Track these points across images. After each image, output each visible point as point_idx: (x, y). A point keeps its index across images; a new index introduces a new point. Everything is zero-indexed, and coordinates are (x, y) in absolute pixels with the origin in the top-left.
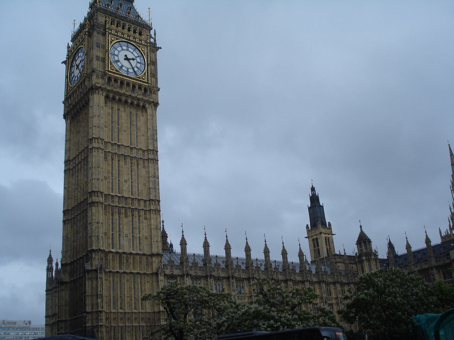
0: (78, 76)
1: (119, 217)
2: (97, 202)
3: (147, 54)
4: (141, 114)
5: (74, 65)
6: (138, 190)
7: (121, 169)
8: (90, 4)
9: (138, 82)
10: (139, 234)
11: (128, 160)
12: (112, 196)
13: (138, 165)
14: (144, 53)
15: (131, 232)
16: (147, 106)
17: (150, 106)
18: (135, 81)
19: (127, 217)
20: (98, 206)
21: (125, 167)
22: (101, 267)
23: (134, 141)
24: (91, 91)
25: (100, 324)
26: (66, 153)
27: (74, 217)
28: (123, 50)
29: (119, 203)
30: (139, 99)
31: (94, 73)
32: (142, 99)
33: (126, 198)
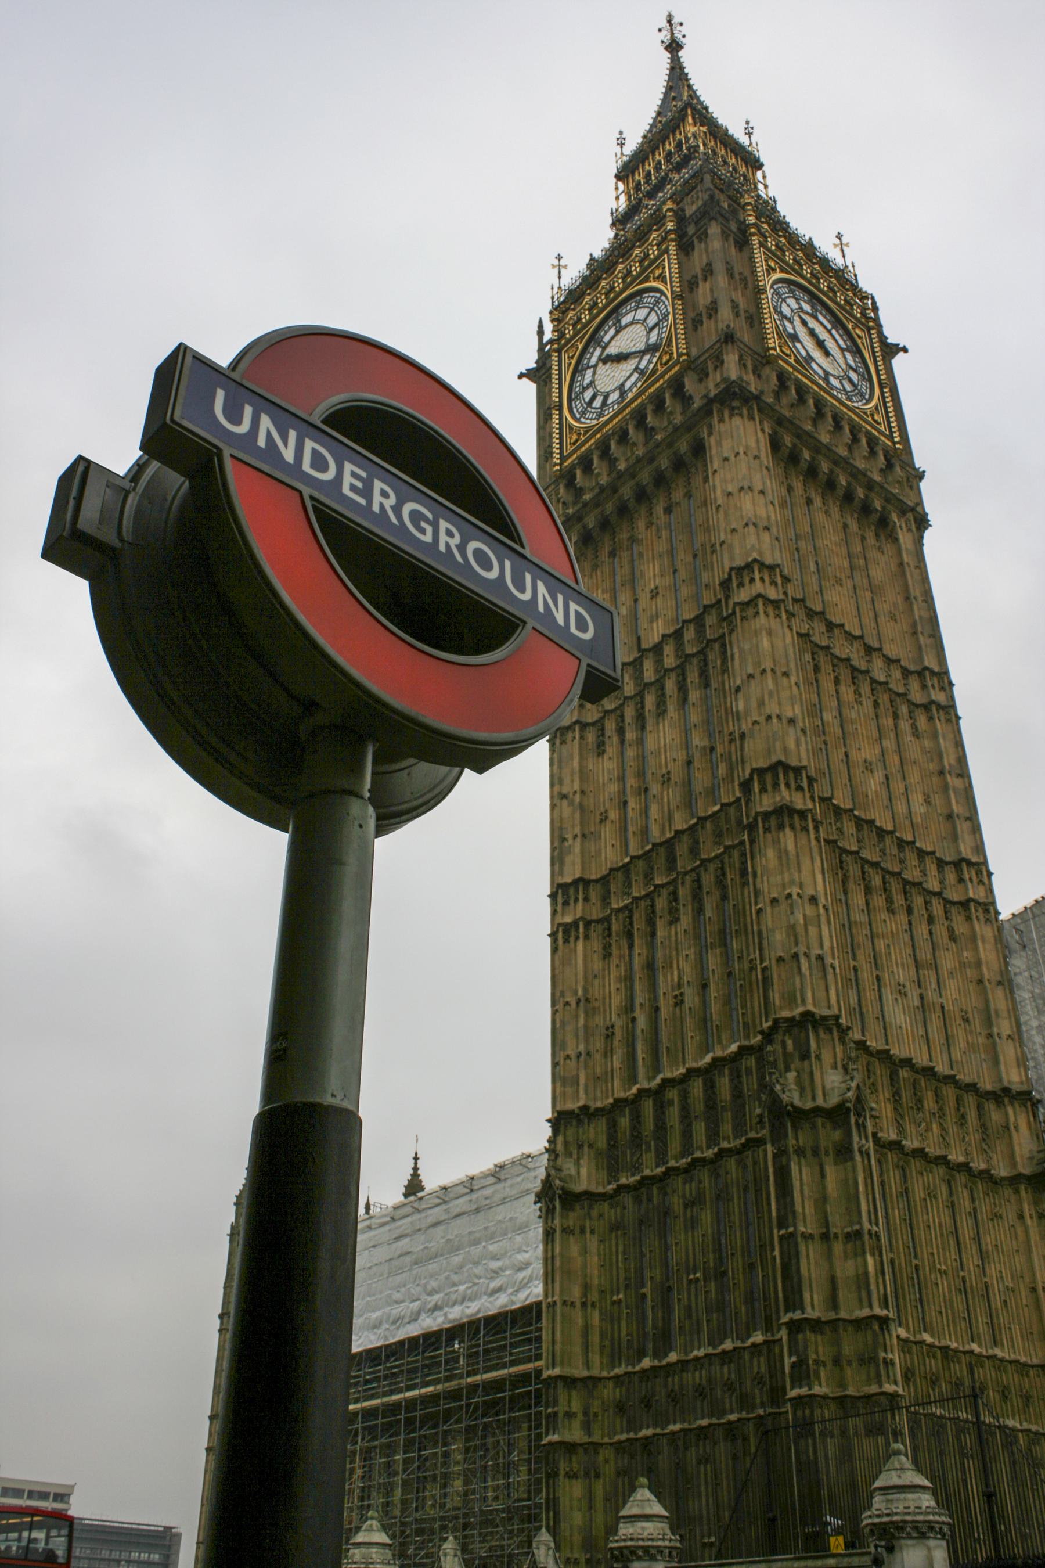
0: (623, 385)
8: (612, 214)
11: (865, 688)
13: (896, 716)
16: (894, 517)
17: (903, 520)
18: (856, 419)
20: (805, 829)
22: (859, 1099)
30: (870, 485)
31: (730, 345)
33: (881, 833)
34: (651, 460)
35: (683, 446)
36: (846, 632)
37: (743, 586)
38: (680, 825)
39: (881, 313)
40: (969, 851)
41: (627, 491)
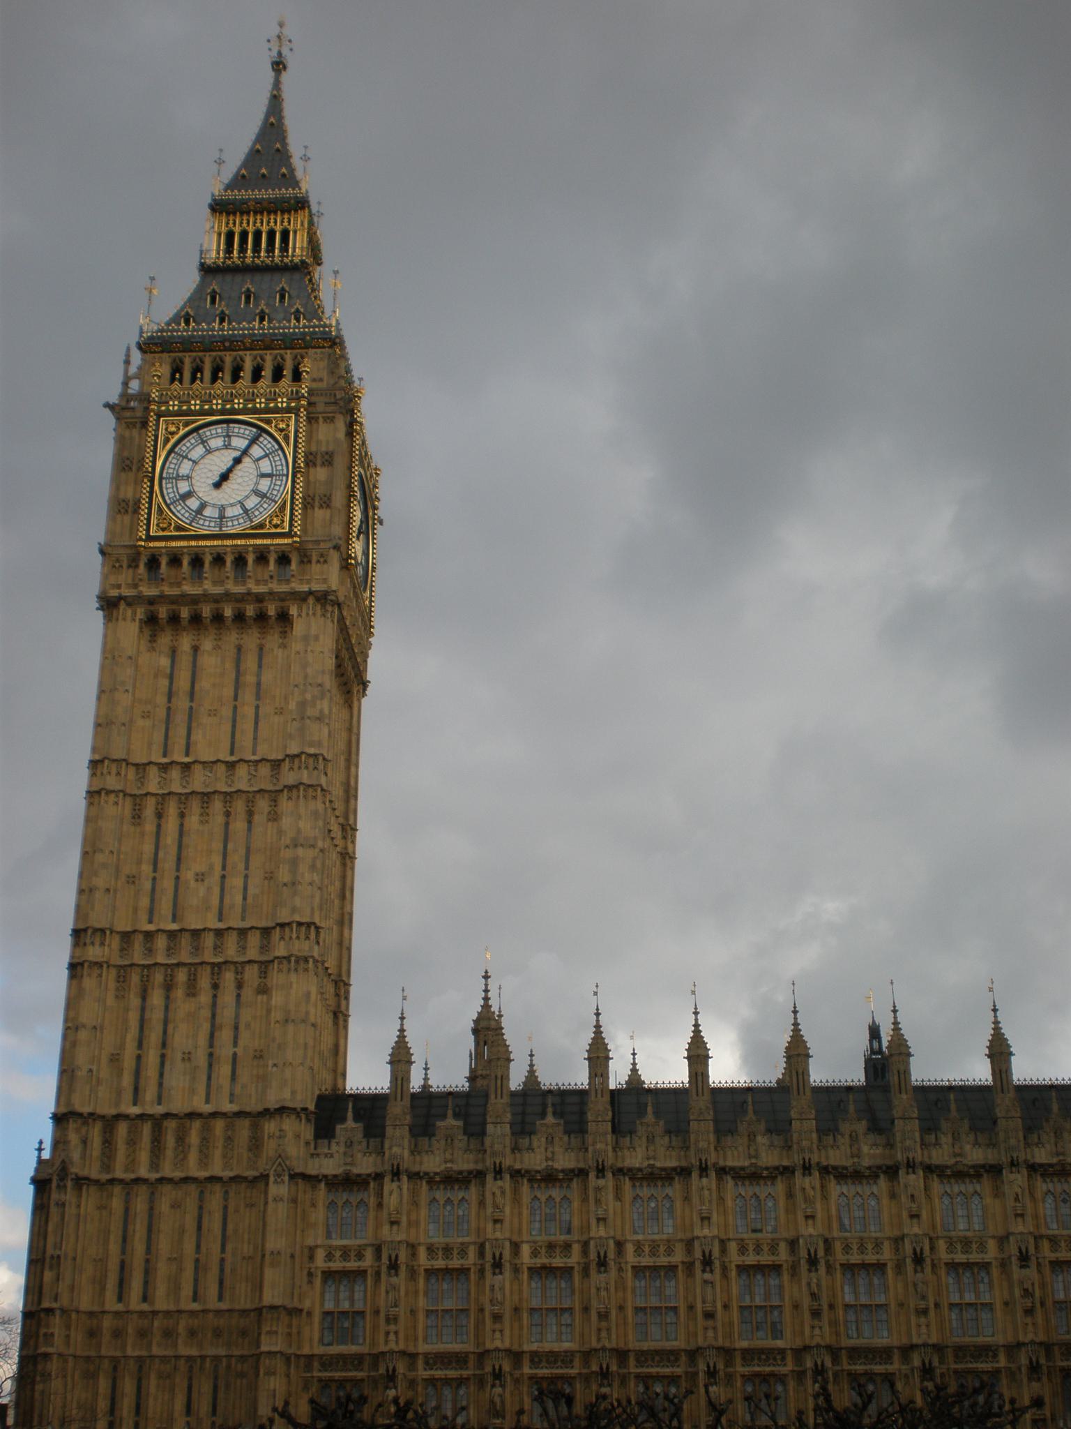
1: (167, 998)
3: (296, 436)
6: (245, 898)
7: (185, 839)
9: (252, 542)
10: (235, 1044)
12: (149, 936)
13: (250, 814)
15: (202, 1041)
19: (194, 995)
21: (203, 832)
23: (245, 740)
25: (43, 1350)
28: (209, 451)
29: (170, 951)
30: (259, 598)
32: (271, 593)
33: (196, 933)
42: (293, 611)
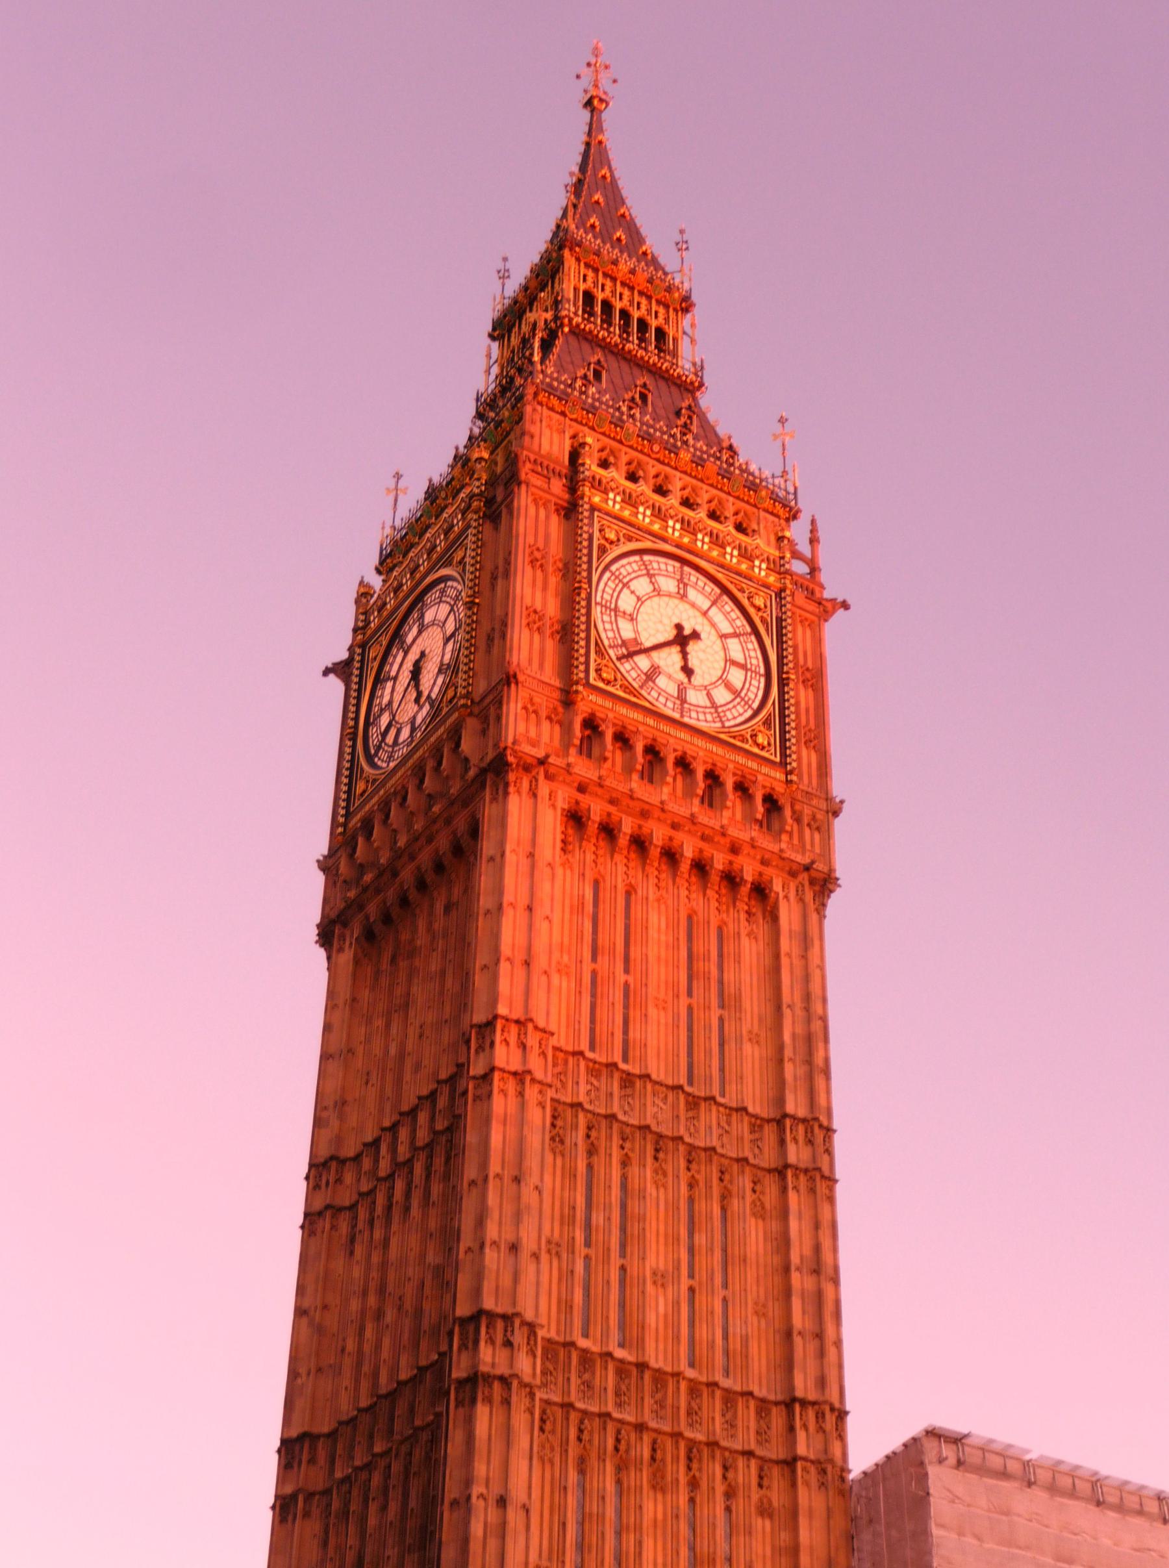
0: (414, 717)
2: (504, 1380)
3: (780, 628)
4: (744, 927)
5: (393, 673)
6: (726, 1337)
7: (634, 1206)
8: (477, 400)
11: (676, 1162)
14: (763, 620)
17: (792, 886)
20: (506, 1402)
21: (659, 1198)
24: (490, 778)
26: (318, 1123)
27: (347, 1479)
28: (657, 592)
30: (735, 849)
31: (513, 686)
33: (660, 1378)
34: (430, 840)
35: (461, 824)
36: (656, 1083)
37: (483, 1050)
38: (403, 1376)
39: (822, 549)
40: (811, 1383)
41: (407, 875)
42: (777, 886)
